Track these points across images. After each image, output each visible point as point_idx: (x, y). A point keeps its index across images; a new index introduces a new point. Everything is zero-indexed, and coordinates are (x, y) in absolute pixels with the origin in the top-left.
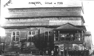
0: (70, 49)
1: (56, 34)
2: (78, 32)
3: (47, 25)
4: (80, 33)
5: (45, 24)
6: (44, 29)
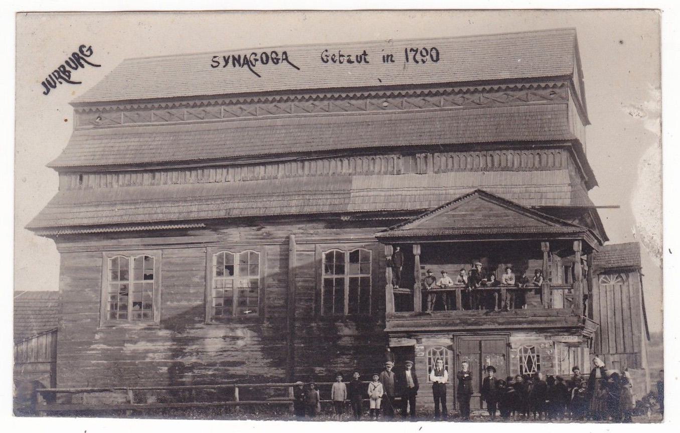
0: (490, 368)
1: (395, 270)
2: (542, 251)
3: (337, 210)
4: (561, 255)
5: (323, 205)
6: (319, 232)
